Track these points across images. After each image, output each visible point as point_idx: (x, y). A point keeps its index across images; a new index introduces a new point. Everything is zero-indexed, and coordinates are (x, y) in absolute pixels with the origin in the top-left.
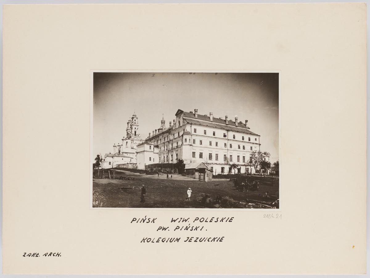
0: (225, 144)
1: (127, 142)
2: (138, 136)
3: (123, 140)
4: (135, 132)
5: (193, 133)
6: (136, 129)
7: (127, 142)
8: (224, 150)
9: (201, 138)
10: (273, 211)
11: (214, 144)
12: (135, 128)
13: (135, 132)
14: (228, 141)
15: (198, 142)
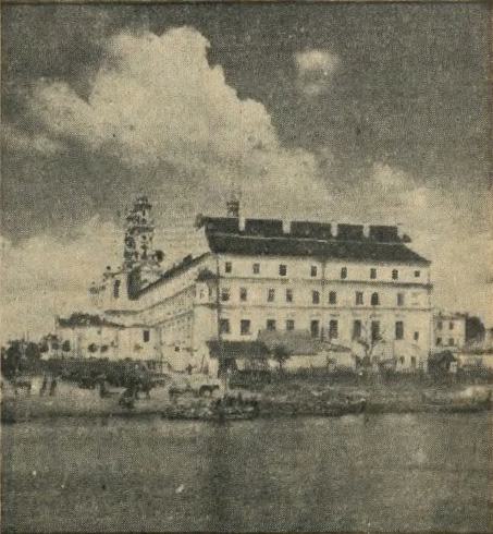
4: (144, 247)
11: (280, 295)
13: (144, 247)
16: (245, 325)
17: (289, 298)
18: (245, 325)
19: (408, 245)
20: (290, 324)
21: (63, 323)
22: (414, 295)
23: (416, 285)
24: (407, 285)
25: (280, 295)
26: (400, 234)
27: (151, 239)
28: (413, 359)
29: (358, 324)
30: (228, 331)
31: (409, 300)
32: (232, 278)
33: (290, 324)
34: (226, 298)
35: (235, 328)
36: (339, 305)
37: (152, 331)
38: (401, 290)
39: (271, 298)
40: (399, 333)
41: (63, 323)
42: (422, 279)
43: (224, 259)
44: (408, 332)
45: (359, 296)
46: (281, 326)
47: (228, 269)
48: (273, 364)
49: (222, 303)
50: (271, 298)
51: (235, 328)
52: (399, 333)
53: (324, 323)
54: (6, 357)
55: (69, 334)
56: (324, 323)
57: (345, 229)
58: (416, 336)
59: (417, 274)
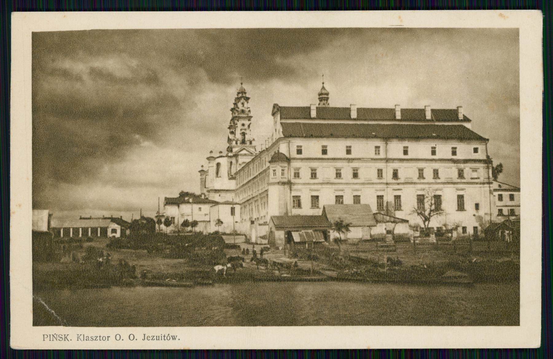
0: (380, 172)
1: (218, 165)
2: (251, 143)
3: (208, 159)
4: (244, 134)
5: (294, 154)
6: (246, 127)
7: (218, 165)
8: (375, 186)
9: (314, 164)
10: (519, 326)
11: (347, 174)
12: (243, 125)
13: (244, 134)
14: (388, 164)
15: (305, 174)
16: (315, 199)
17: (355, 175)
18: (315, 199)
19: (468, 125)
20: (357, 199)
21: (169, 202)
22: (475, 170)
23: (475, 161)
24: (466, 161)
25: (347, 174)
26: (461, 117)
27: (249, 126)
28: (475, 228)
29: (421, 199)
30: (299, 206)
31: (468, 173)
32: (302, 159)
33: (357, 199)
34: (297, 175)
35: (306, 201)
36: (402, 180)
37: (238, 208)
38: (462, 166)
39: (338, 175)
40: (461, 207)
41: (169, 202)
42: (481, 155)
43: (297, 142)
44: (469, 206)
45: (421, 171)
46: (348, 200)
47: (299, 152)
48: (334, 234)
49: (293, 181)
50: (338, 175)
51: (306, 201)
52: (461, 207)
53: (389, 198)
54: (128, 232)
55: (172, 211)
56: (389, 198)
57: (408, 114)
58: (477, 206)
59: (476, 150)
